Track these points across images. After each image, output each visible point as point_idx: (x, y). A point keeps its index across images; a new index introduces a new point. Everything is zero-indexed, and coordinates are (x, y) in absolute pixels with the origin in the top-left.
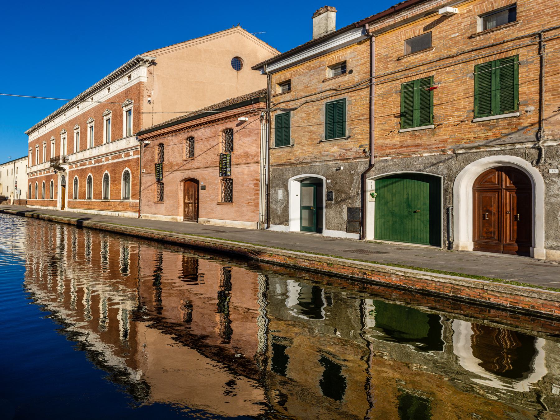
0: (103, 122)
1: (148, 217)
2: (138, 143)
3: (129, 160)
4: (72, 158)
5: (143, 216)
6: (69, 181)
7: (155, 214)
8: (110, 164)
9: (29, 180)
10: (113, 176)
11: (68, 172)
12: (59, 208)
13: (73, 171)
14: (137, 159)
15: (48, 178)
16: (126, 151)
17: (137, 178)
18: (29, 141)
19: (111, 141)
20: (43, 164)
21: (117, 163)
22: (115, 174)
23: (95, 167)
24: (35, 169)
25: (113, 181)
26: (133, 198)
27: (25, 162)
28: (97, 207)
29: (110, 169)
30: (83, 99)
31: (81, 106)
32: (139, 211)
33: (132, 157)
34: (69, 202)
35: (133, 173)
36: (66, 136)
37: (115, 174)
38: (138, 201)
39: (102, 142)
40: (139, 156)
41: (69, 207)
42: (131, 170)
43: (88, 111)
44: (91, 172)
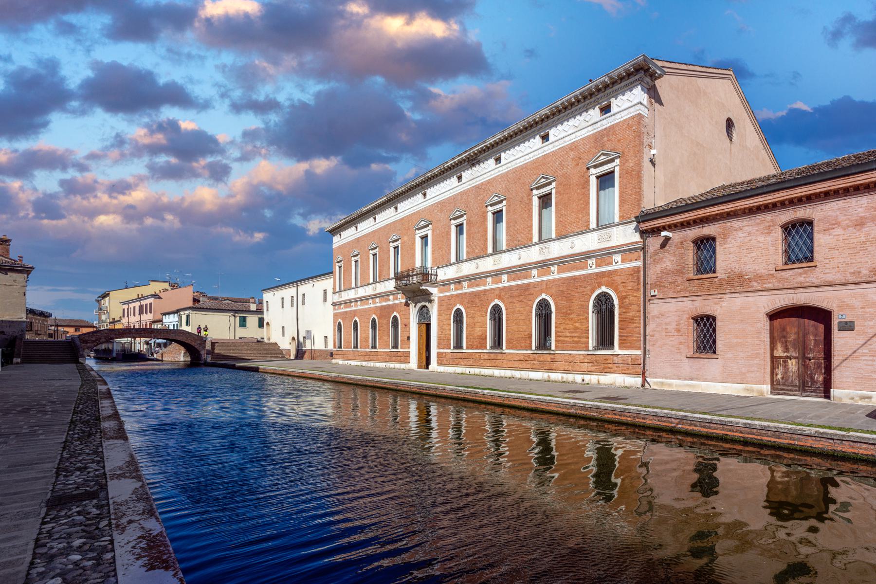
0: (531, 200)
1: (670, 385)
2: (637, 237)
3: (611, 273)
4: (445, 274)
5: (656, 383)
6: (440, 314)
7: (692, 379)
8: (553, 281)
9: (336, 316)
10: (563, 303)
11: (436, 299)
12: (413, 364)
13: (452, 296)
14: (636, 270)
15: (384, 311)
16: (604, 255)
17: (634, 307)
18: (334, 246)
19: (554, 236)
20: (371, 286)
21: (574, 279)
22: (568, 301)
23: (510, 288)
24: (351, 295)
25: (564, 313)
26: (621, 347)
27: (327, 284)
28: (516, 364)
29: (553, 291)
30: (473, 161)
31: (467, 175)
32: (644, 373)
33: (618, 263)
34: (439, 354)
35: (621, 299)
36: (430, 233)
37: (568, 301)
38: (639, 352)
39: (531, 239)
40: (639, 263)
41: (440, 364)
42: (616, 290)
43: (489, 182)
44: (500, 298)
